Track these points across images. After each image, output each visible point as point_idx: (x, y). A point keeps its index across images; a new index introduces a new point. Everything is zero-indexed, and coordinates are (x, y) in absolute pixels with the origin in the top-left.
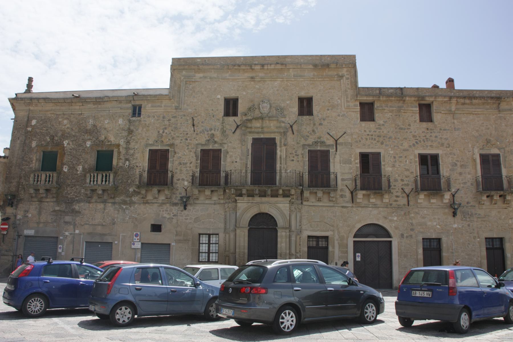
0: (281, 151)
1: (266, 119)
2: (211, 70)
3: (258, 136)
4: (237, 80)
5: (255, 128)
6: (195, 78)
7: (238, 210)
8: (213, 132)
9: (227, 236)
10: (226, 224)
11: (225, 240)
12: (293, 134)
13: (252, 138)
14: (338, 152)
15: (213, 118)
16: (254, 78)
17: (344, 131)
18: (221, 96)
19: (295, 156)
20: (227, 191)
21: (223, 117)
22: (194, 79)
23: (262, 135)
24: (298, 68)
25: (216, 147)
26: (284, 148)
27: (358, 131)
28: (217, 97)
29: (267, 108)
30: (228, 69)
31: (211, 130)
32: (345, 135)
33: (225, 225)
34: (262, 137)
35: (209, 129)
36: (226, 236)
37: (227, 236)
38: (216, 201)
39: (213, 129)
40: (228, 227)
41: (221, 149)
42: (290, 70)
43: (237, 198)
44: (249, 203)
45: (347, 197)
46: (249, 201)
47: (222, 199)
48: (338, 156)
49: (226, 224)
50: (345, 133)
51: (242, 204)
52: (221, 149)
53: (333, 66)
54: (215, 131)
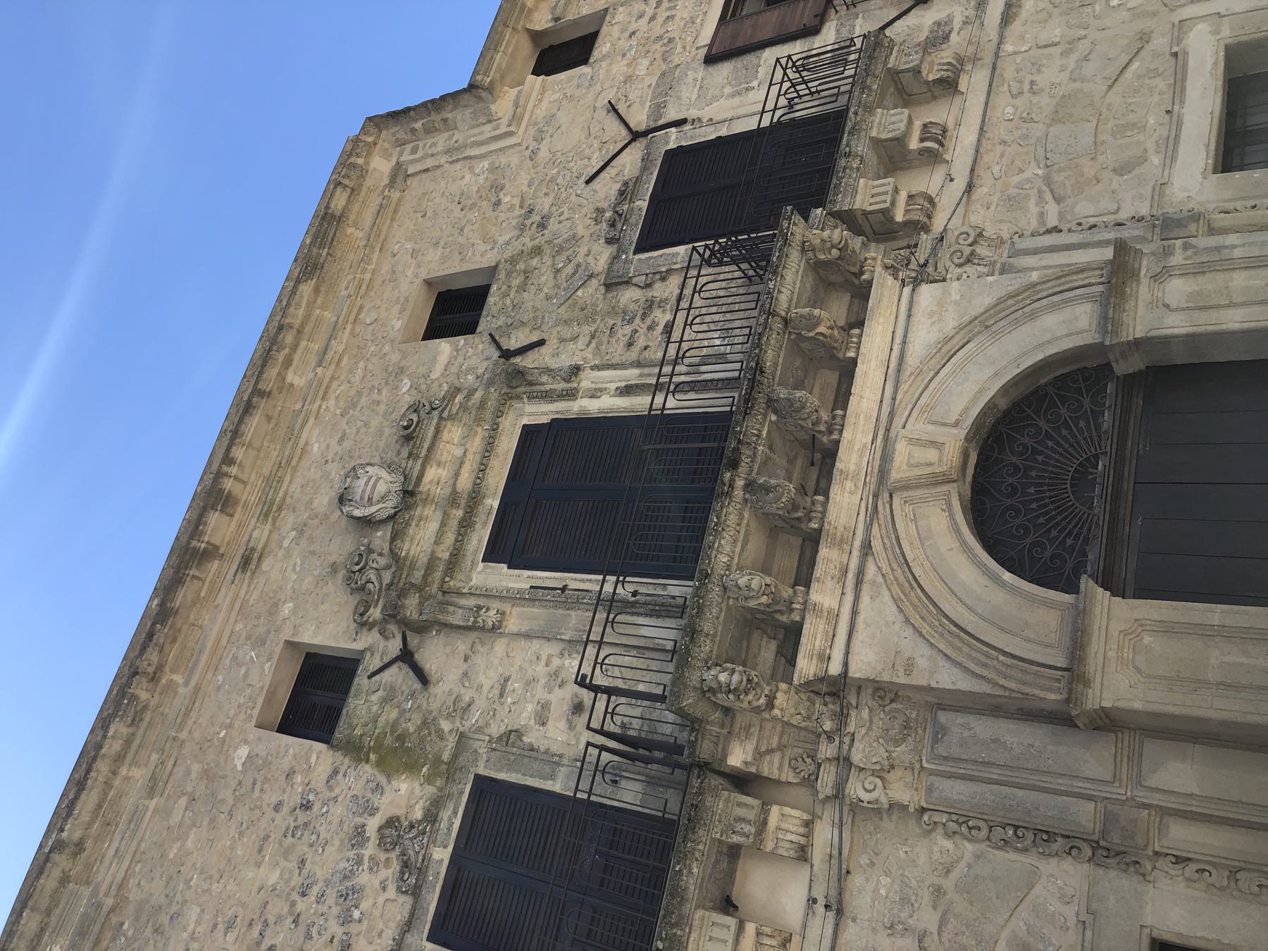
0: (594, 394)
1: (415, 474)
2: (117, 783)
3: (485, 524)
4: (224, 642)
5: (437, 542)
6: (103, 890)
7: (908, 673)
8: (373, 824)
9: (1180, 835)
10: (1051, 836)
11: (1234, 873)
12: (541, 343)
13: (481, 565)
14: (692, 113)
15: (316, 808)
16: (253, 549)
17: (601, 114)
18: (246, 742)
19: (648, 321)
20: (737, 758)
21: (332, 747)
22: (106, 895)
23: (489, 501)
24: (295, 347)
25: (455, 813)
26: (587, 380)
27: (625, 62)
28: (239, 765)
29: (378, 479)
30: (154, 678)
31: (360, 831)
32: (621, 108)
33: (1059, 844)
34: (496, 504)
35: (351, 854)
36: (1179, 860)
37: (1180, 835)
38: (819, 893)
39: (359, 820)
40: (1085, 815)
41: (477, 777)
42: (291, 385)
43: (806, 667)
44: (860, 573)
45: (948, 16)
46: (851, 575)
47: (808, 824)
48: (706, 113)
49: (1051, 836)
50: (613, 108)
51: (860, 635)
52: (477, 777)
53: (339, 201)
54: (373, 811)
